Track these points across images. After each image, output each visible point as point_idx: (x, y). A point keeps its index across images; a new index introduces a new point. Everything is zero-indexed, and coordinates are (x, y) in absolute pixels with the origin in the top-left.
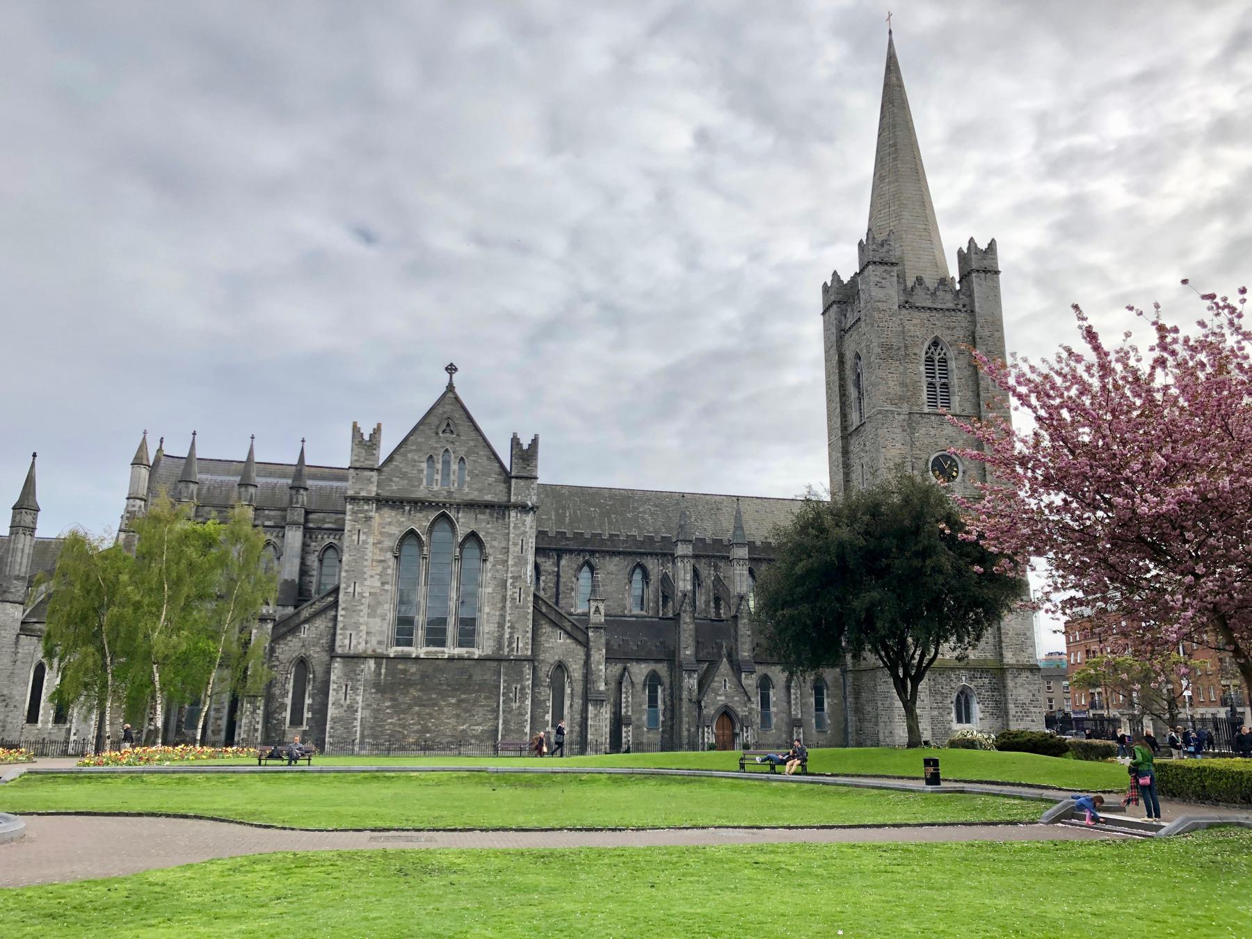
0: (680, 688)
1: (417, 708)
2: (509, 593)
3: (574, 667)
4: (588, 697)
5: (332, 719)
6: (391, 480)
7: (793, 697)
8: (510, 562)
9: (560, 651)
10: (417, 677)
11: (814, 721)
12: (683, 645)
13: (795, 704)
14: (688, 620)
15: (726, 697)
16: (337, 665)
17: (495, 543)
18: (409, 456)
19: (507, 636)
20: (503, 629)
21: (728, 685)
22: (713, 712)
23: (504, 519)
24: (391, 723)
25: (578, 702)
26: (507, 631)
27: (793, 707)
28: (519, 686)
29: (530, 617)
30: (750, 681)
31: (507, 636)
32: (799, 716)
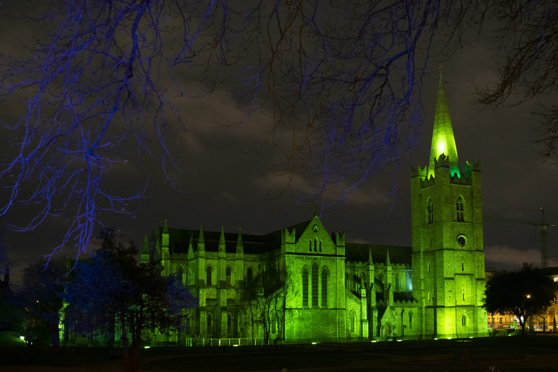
0: (372, 317)
1: (311, 326)
2: (338, 288)
3: (357, 312)
4: (362, 321)
5: (287, 330)
6: (299, 248)
7: (404, 318)
8: (338, 277)
9: (352, 307)
10: (311, 316)
11: (409, 326)
12: (372, 302)
13: (405, 320)
14: (374, 293)
15: (389, 319)
16: (287, 313)
17: (332, 271)
18: (304, 239)
19: (338, 302)
20: (337, 300)
21: (389, 315)
22: (384, 324)
23: (335, 262)
24: (304, 331)
25: (359, 323)
26: (338, 300)
27: (404, 322)
28: (342, 319)
29: (344, 295)
30: (394, 314)
31: (338, 302)
32: (405, 324)
